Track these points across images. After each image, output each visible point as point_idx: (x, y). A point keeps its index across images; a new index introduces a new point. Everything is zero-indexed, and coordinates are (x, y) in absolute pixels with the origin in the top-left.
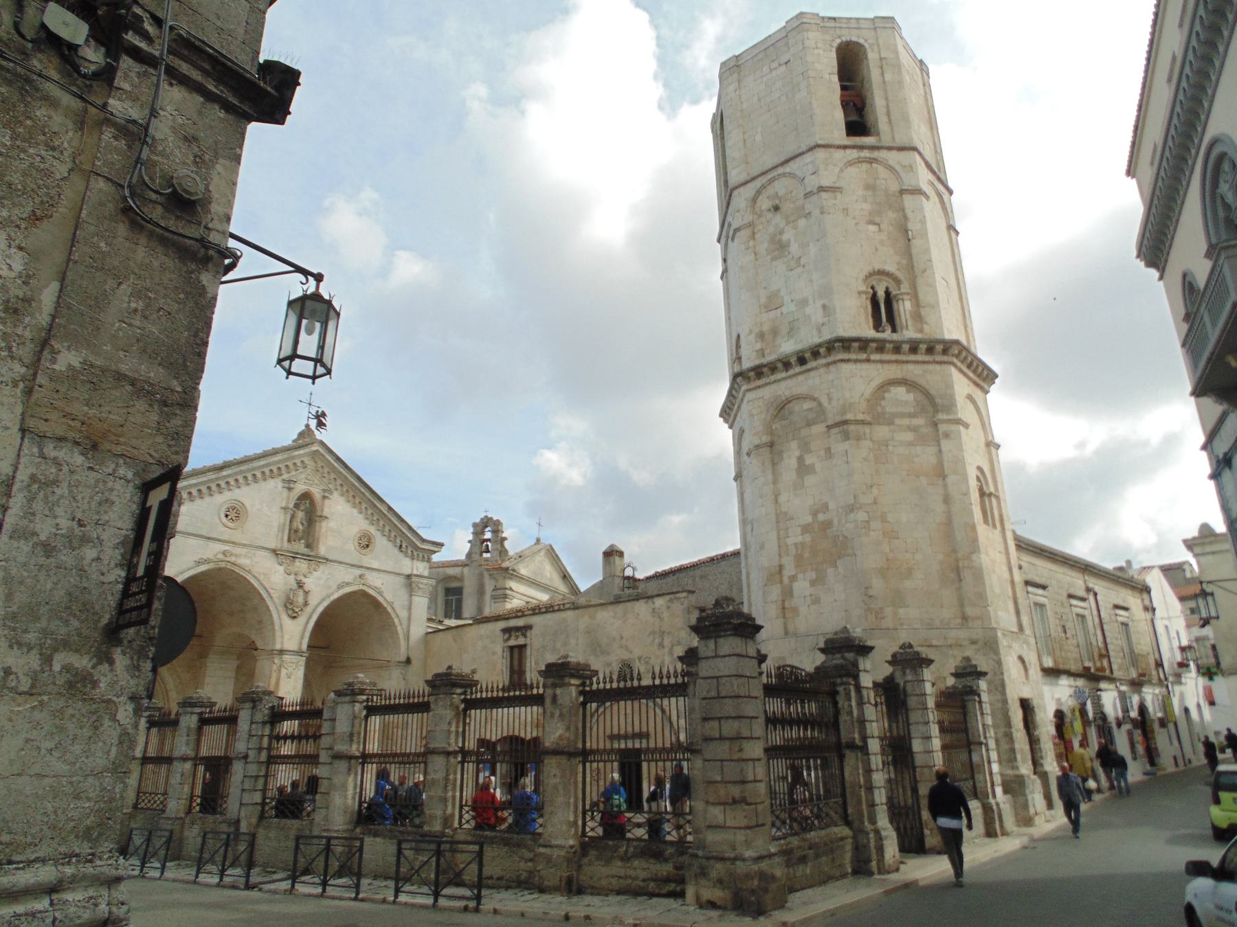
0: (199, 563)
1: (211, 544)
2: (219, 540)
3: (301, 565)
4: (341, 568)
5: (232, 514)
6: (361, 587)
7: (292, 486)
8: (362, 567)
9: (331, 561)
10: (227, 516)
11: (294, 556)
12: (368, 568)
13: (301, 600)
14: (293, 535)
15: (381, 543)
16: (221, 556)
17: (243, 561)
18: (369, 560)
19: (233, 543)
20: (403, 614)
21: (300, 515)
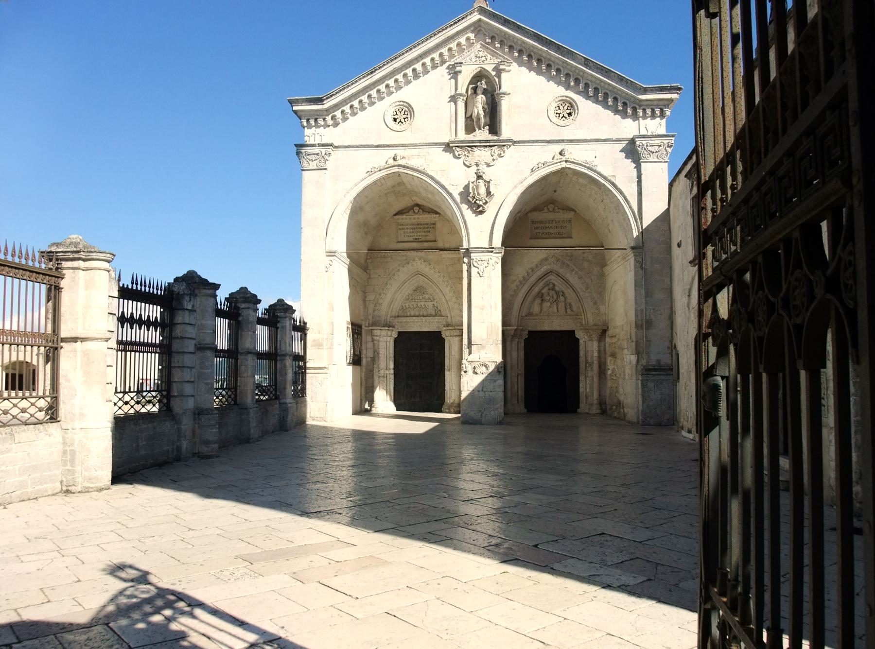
0: (370, 173)
1: (382, 151)
2: (388, 146)
3: (482, 155)
4: (537, 148)
5: (400, 117)
6: (564, 165)
7: (458, 69)
8: (563, 141)
9: (519, 142)
10: (395, 120)
11: (471, 146)
12: (571, 141)
13: (483, 191)
14: (471, 125)
15: (585, 106)
16: (391, 162)
17: (414, 163)
18: (573, 129)
19: (403, 145)
20: (630, 191)
21: (481, 99)
